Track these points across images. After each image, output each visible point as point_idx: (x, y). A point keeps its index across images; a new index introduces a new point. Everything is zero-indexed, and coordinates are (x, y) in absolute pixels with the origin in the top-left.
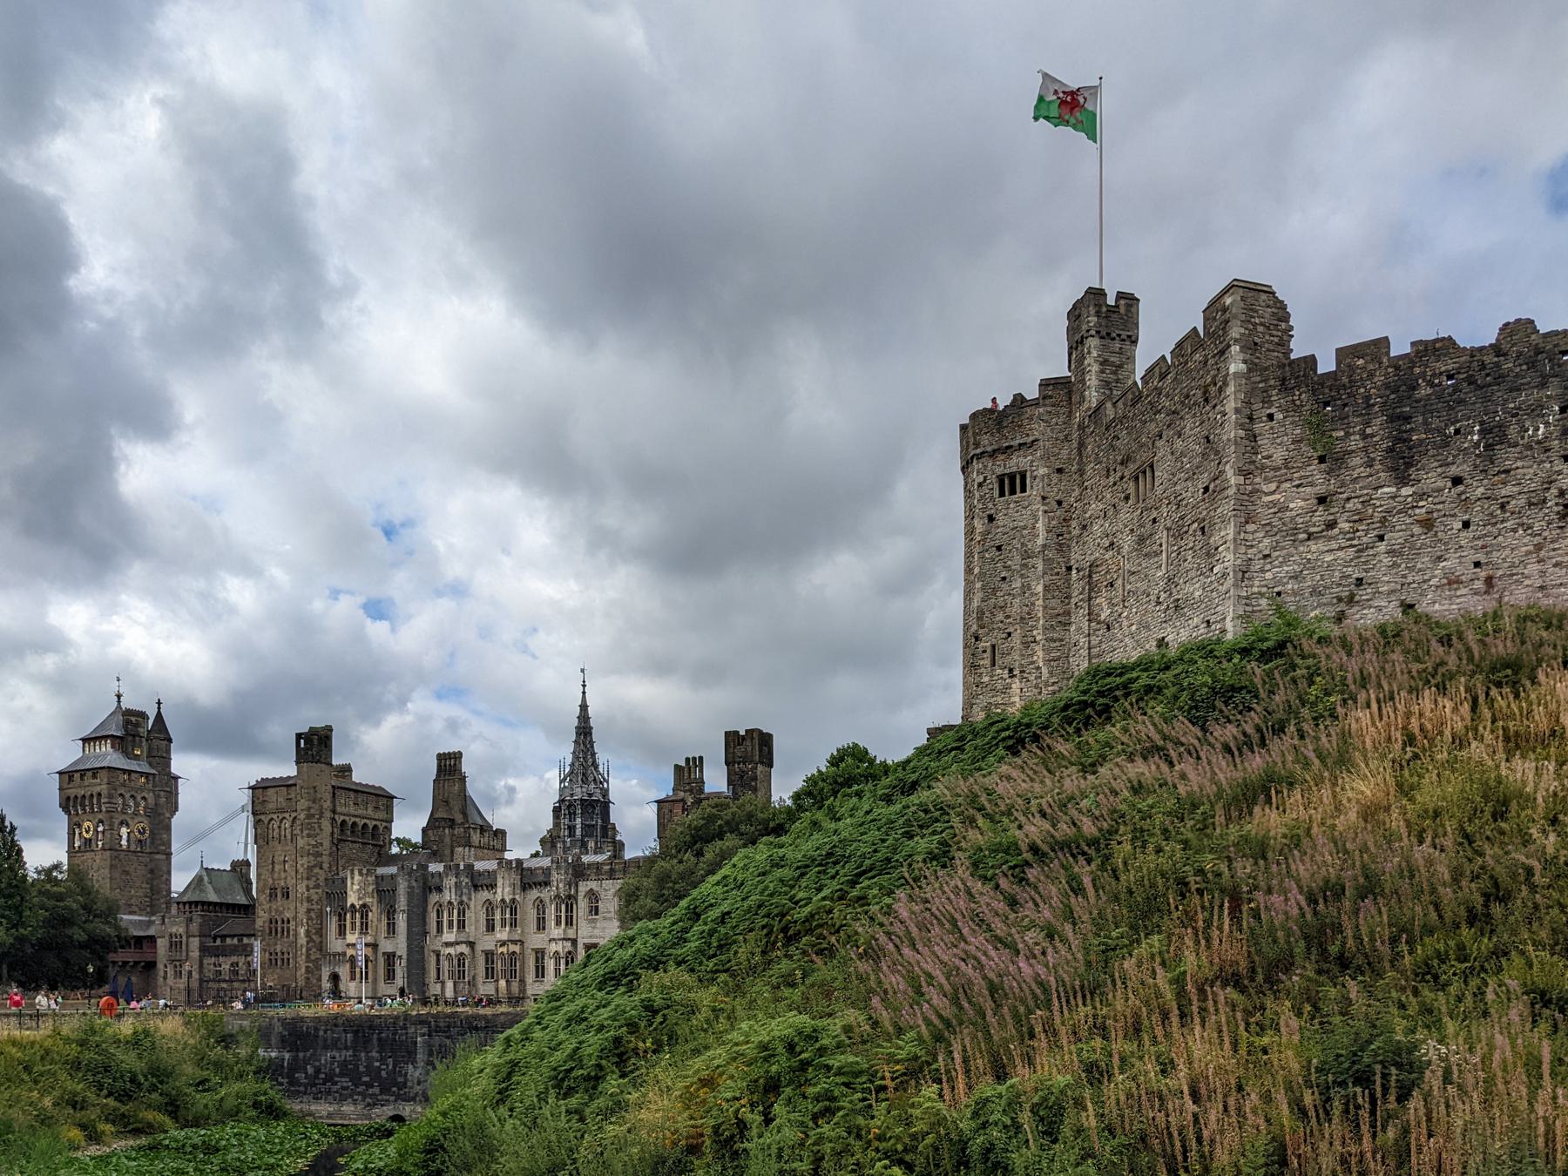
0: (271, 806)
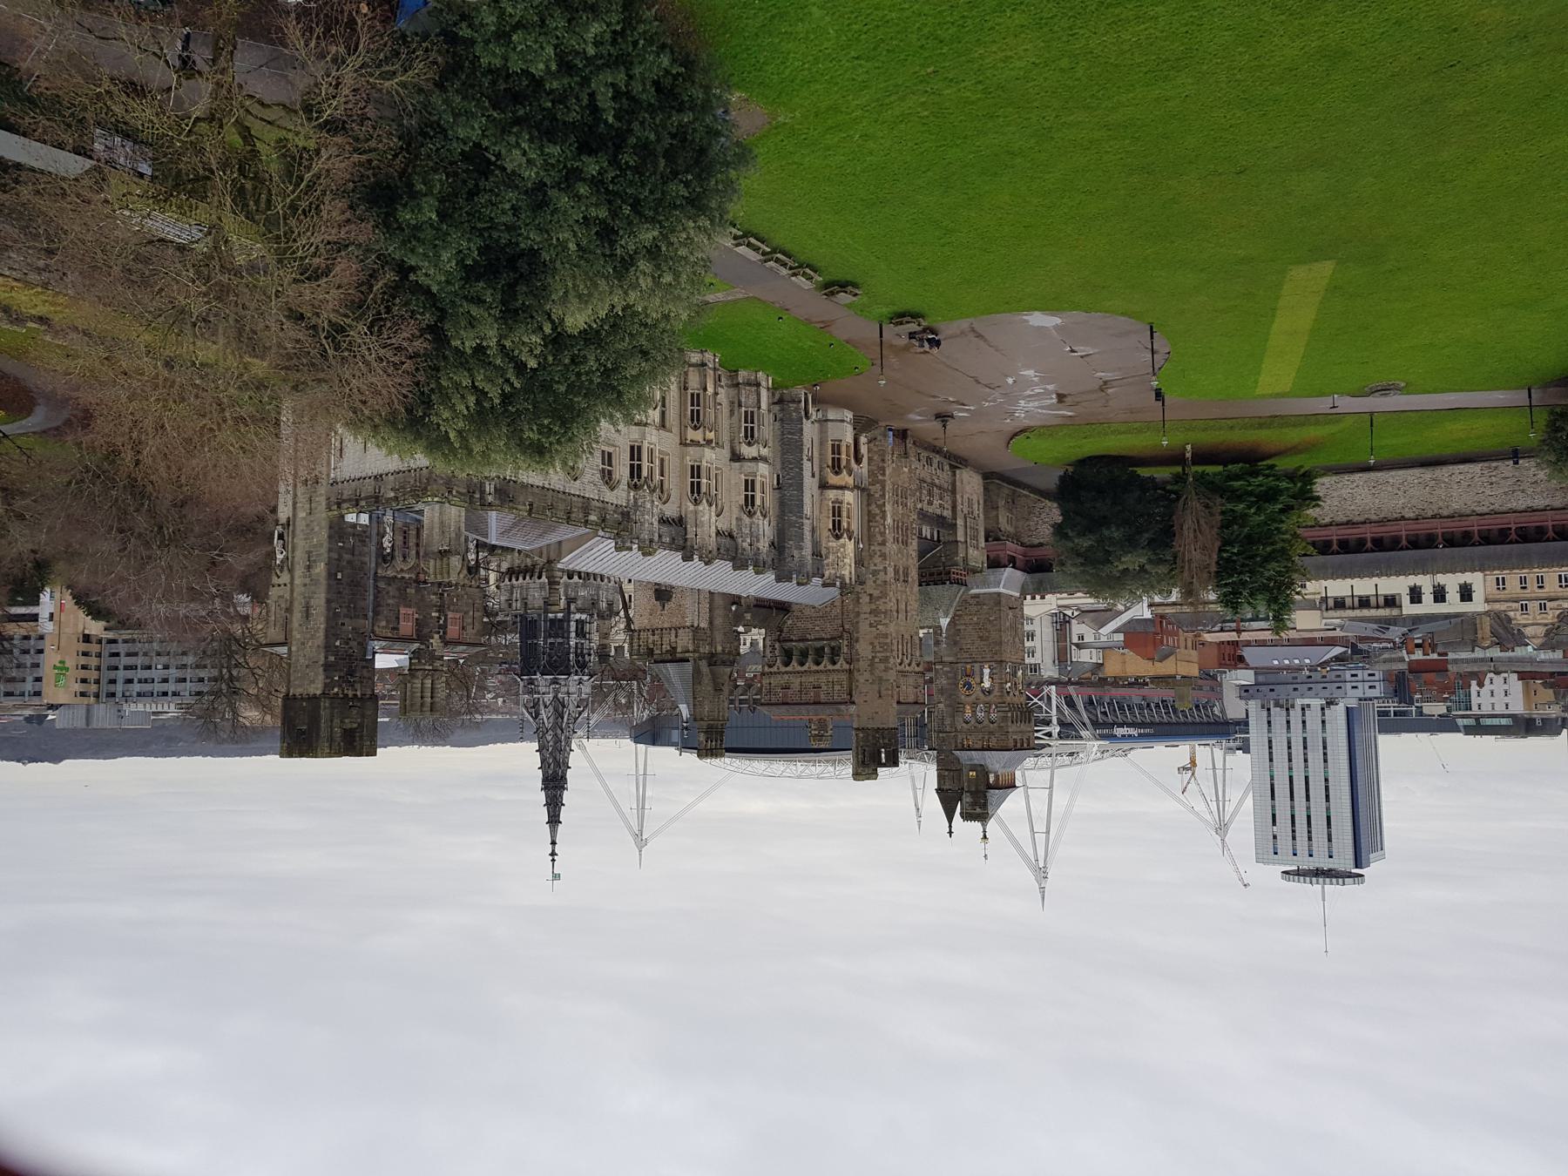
0: (911, 681)
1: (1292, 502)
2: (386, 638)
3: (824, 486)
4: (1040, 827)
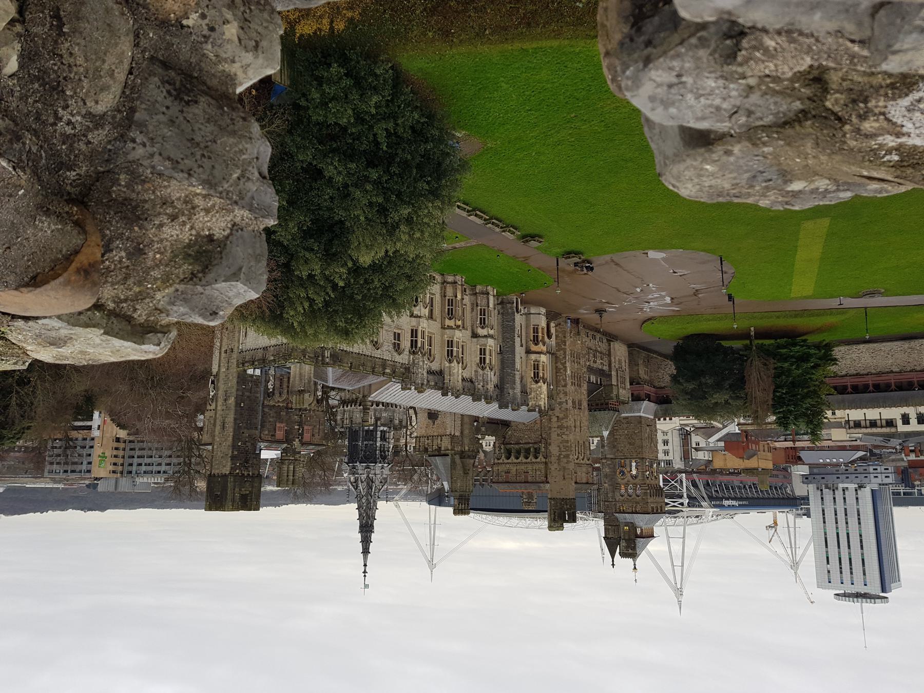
0: (584, 469)
1: (820, 362)
2: (267, 441)
3: (528, 352)
4: (678, 563)
